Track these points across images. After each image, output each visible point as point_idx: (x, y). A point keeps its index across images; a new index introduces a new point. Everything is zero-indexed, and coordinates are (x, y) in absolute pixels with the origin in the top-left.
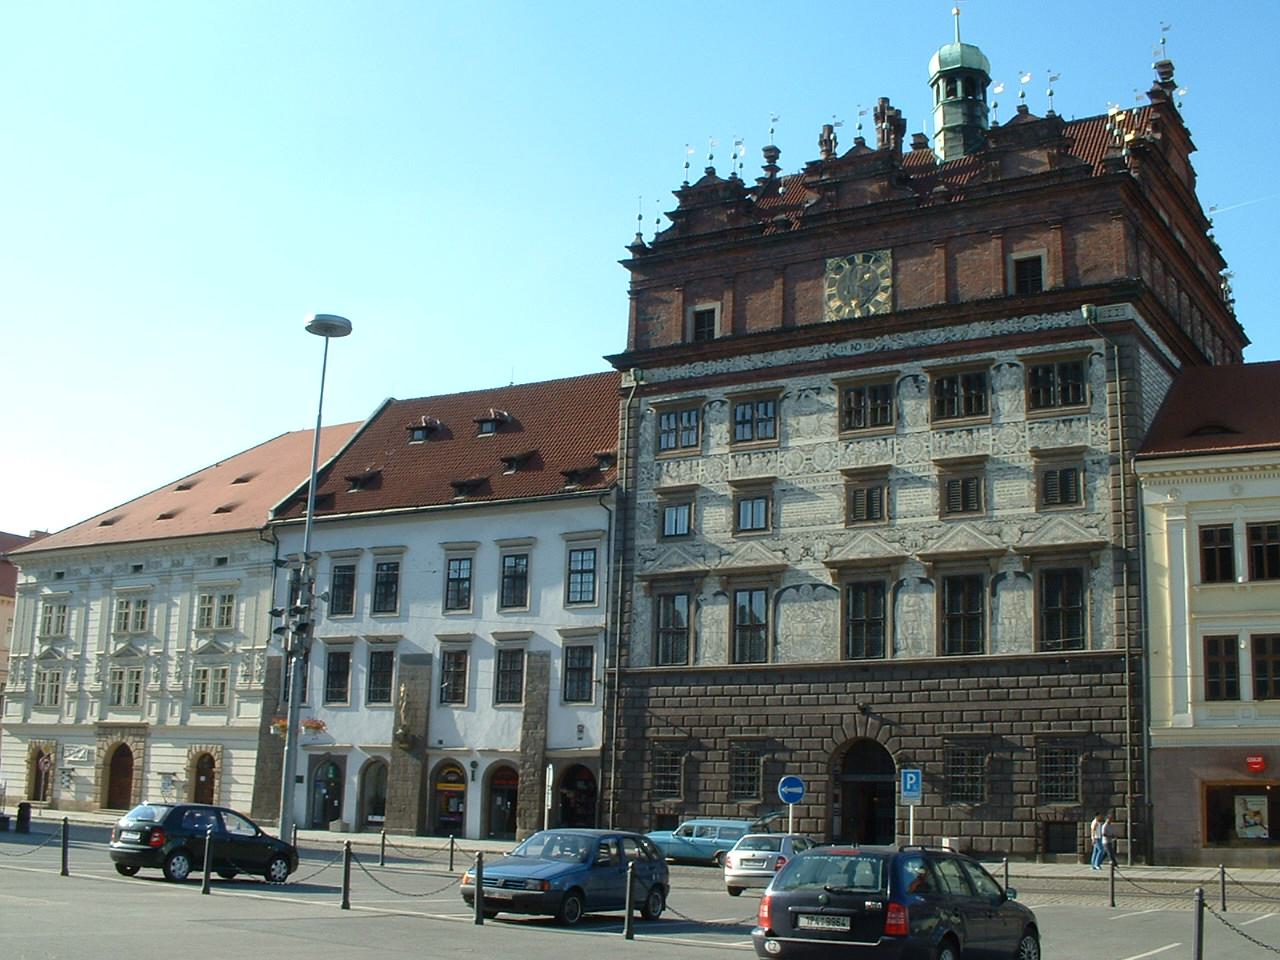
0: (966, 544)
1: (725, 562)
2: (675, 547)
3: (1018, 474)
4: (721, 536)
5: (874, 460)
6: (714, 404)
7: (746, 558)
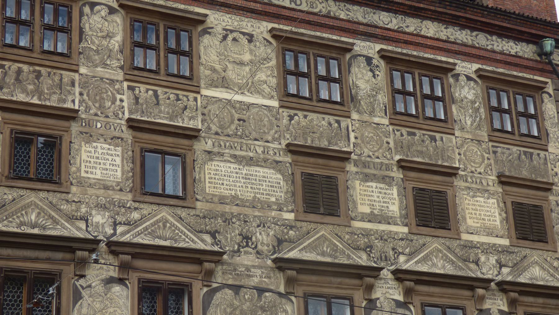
0: (444, 267)
1: (123, 234)
2: (32, 197)
3: (488, 199)
4: (117, 197)
5: (326, 143)
6: (98, 8)
7: (160, 232)
